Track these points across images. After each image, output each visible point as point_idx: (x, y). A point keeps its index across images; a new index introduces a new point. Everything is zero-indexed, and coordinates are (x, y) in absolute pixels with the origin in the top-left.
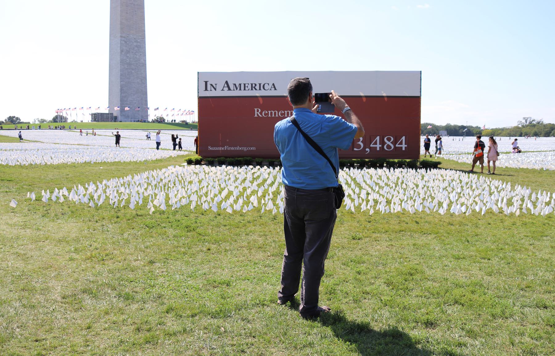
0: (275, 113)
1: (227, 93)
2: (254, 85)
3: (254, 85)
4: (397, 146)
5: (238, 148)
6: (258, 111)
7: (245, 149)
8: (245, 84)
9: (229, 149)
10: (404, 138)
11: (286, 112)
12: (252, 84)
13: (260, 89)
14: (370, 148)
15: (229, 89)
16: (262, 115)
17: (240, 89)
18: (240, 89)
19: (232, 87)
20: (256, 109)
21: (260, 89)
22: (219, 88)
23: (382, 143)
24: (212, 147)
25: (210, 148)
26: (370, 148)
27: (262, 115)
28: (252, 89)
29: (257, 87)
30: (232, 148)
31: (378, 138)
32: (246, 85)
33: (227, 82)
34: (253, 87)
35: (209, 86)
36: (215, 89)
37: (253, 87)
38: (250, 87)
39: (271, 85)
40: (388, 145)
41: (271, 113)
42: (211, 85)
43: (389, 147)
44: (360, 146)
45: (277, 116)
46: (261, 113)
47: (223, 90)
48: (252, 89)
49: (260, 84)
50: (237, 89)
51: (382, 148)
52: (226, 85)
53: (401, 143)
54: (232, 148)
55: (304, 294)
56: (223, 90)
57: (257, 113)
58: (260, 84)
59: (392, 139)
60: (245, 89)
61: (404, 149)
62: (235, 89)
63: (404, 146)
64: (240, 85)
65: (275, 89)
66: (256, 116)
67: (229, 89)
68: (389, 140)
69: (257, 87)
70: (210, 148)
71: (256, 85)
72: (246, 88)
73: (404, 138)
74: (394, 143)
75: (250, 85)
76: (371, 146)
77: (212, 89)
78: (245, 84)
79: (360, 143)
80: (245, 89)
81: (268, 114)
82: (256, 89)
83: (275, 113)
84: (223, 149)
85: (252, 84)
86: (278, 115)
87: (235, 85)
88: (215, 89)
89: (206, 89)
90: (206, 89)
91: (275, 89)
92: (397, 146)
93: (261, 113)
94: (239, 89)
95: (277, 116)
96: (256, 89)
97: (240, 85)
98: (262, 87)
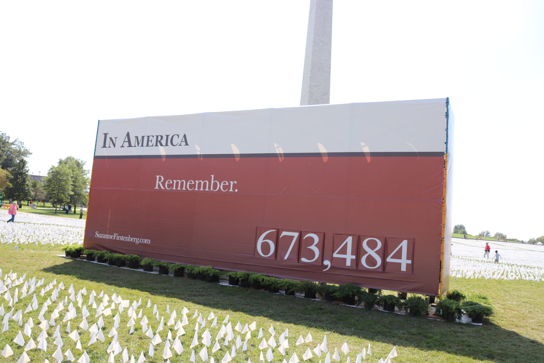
2: (159, 138)
3: (159, 138)
4: (389, 260)
8: (148, 137)
12: (157, 136)
13: (167, 145)
14: (332, 259)
15: (130, 145)
17: (142, 146)
18: (142, 146)
19: (133, 141)
20: (158, 177)
21: (167, 145)
22: (119, 143)
23: (358, 251)
26: (332, 259)
28: (156, 145)
29: (164, 142)
31: (349, 240)
32: (151, 138)
36: (114, 145)
39: (181, 136)
40: (370, 256)
42: (111, 139)
43: (371, 261)
44: (312, 254)
46: (163, 184)
47: (122, 146)
48: (156, 145)
49: (167, 136)
50: (138, 144)
51: (357, 261)
53: (398, 255)
56: (122, 146)
57: (160, 183)
58: (167, 136)
59: (379, 245)
60: (148, 145)
62: (136, 145)
63: (404, 262)
64: (143, 137)
65: (187, 144)
67: (130, 145)
68: (372, 245)
69: (164, 142)
71: (162, 137)
72: (150, 144)
74: (384, 254)
75: (155, 137)
76: (335, 255)
77: (112, 145)
78: (148, 137)
79: (313, 248)
82: (161, 145)
85: (157, 136)
86: (186, 187)
87: (137, 137)
92: (389, 260)
94: (140, 144)
95: (184, 189)
96: (161, 145)
97: (143, 137)
98: (170, 140)
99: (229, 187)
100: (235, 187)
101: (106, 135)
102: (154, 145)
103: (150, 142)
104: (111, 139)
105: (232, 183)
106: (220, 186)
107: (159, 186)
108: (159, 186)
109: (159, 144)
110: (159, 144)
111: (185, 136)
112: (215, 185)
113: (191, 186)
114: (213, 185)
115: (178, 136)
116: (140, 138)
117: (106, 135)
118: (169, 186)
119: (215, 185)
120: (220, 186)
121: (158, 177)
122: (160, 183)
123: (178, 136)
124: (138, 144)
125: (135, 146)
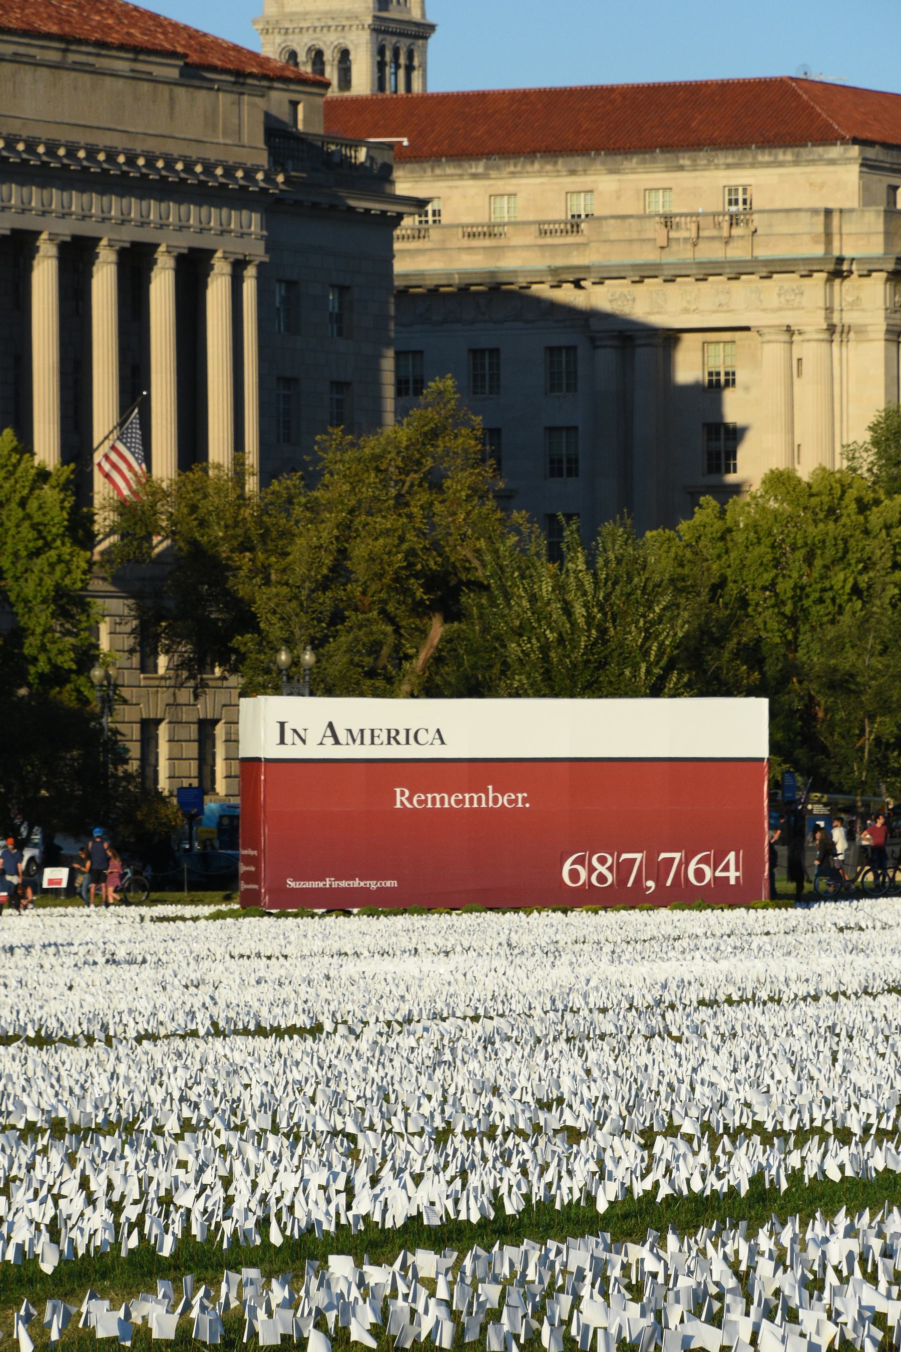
0: (442, 799)
1: (330, 752)
2: (393, 734)
5: (356, 883)
6: (403, 794)
7: (373, 885)
9: (335, 885)
10: (732, 856)
11: (467, 796)
15: (337, 742)
16: (411, 803)
19: (342, 736)
20: (398, 790)
22: (313, 737)
24: (295, 880)
25: (291, 884)
27: (411, 803)
29: (402, 738)
30: (344, 884)
32: (376, 733)
33: (330, 725)
34: (392, 737)
35: (289, 734)
37: (392, 737)
38: (384, 736)
39: (432, 731)
41: (434, 799)
42: (295, 731)
45: (446, 806)
46: (410, 799)
49: (408, 731)
52: (329, 733)
54: (344, 884)
55: (212, 909)
57: (402, 798)
58: (408, 731)
61: (732, 882)
64: (362, 731)
66: (398, 806)
69: (402, 738)
70: (291, 884)
71: (397, 732)
72: (376, 740)
73: (732, 856)
75: (385, 733)
81: (426, 801)
83: (442, 799)
84: (321, 885)
87: (350, 731)
88: (304, 741)
89: (282, 742)
90: (282, 742)
93: (410, 799)
94: (358, 741)
97: (362, 731)
99: (516, 801)
100: (524, 800)
101: (282, 725)
104: (295, 731)
105: (520, 796)
106: (503, 800)
107: (402, 803)
108: (402, 803)
111: (438, 731)
112: (495, 800)
113: (458, 802)
114: (490, 799)
116: (356, 733)
117: (282, 725)
118: (420, 802)
119: (495, 800)
120: (503, 800)
121: (398, 790)
122: (402, 798)
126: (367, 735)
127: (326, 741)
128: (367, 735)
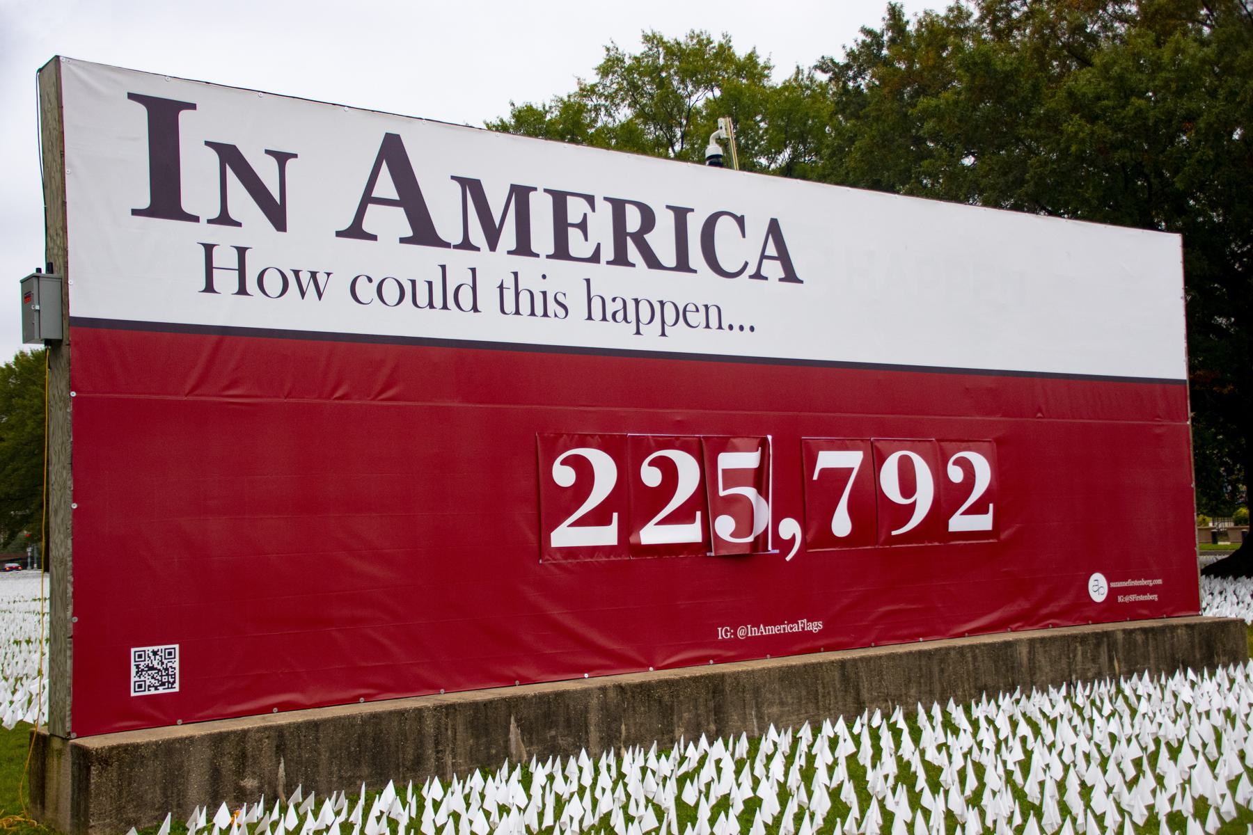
2: (633, 221)
3: (633, 221)
17: (523, 247)
21: (683, 264)
28: (621, 259)
29: (662, 241)
47: (355, 231)
49: (681, 215)
50: (493, 236)
52: (386, 187)
56: (355, 231)
58: (681, 215)
60: (561, 251)
62: (477, 235)
64: (520, 194)
69: (662, 241)
71: (648, 219)
75: (605, 212)
78: (560, 199)
80: (561, 251)
82: (652, 262)
85: (618, 207)
87: (472, 188)
88: (276, 214)
91: (790, 276)
94: (508, 238)
96: (652, 262)
102: (608, 253)
103: (574, 235)
109: (633, 253)
110: (633, 253)
111: (774, 229)
115: (740, 221)
123: (740, 221)
124: (493, 236)
125: (466, 245)
126: (541, 209)
127: (375, 218)
128: (541, 209)
